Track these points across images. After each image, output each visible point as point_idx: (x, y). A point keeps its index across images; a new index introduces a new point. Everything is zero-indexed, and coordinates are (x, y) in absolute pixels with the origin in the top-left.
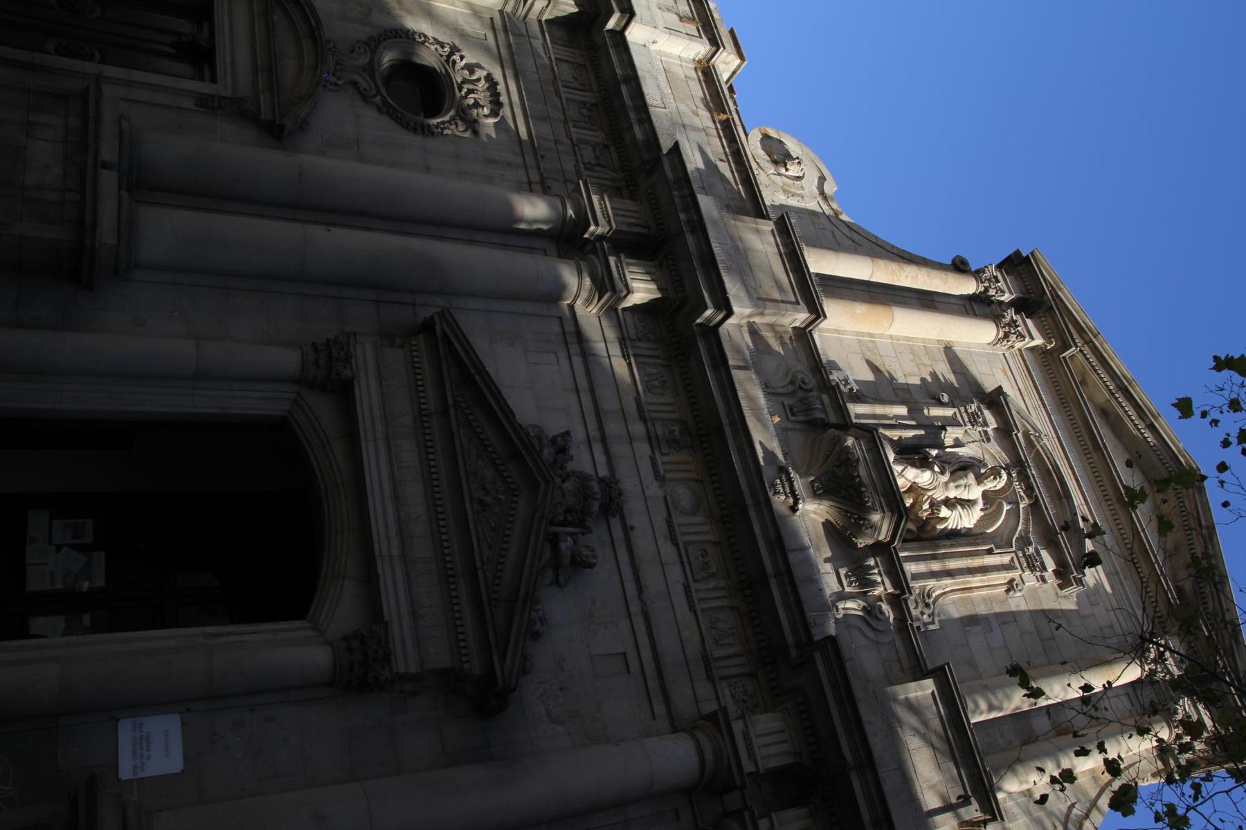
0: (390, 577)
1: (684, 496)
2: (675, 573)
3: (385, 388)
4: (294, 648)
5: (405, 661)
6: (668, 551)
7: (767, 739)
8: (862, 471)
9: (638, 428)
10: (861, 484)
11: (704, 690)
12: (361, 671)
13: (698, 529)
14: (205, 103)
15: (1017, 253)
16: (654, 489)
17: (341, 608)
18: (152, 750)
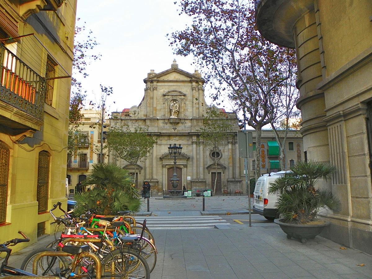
0: (180, 164)
1: (175, 138)
2: (181, 141)
3: (166, 162)
4: (184, 170)
5: (186, 163)
6: (179, 141)
7: (195, 139)
9: (168, 141)
11: (190, 141)
12: (186, 166)
13: (177, 138)
14: (140, 174)
15: (144, 80)
16: (174, 141)
17: (182, 166)
18: (189, 178)
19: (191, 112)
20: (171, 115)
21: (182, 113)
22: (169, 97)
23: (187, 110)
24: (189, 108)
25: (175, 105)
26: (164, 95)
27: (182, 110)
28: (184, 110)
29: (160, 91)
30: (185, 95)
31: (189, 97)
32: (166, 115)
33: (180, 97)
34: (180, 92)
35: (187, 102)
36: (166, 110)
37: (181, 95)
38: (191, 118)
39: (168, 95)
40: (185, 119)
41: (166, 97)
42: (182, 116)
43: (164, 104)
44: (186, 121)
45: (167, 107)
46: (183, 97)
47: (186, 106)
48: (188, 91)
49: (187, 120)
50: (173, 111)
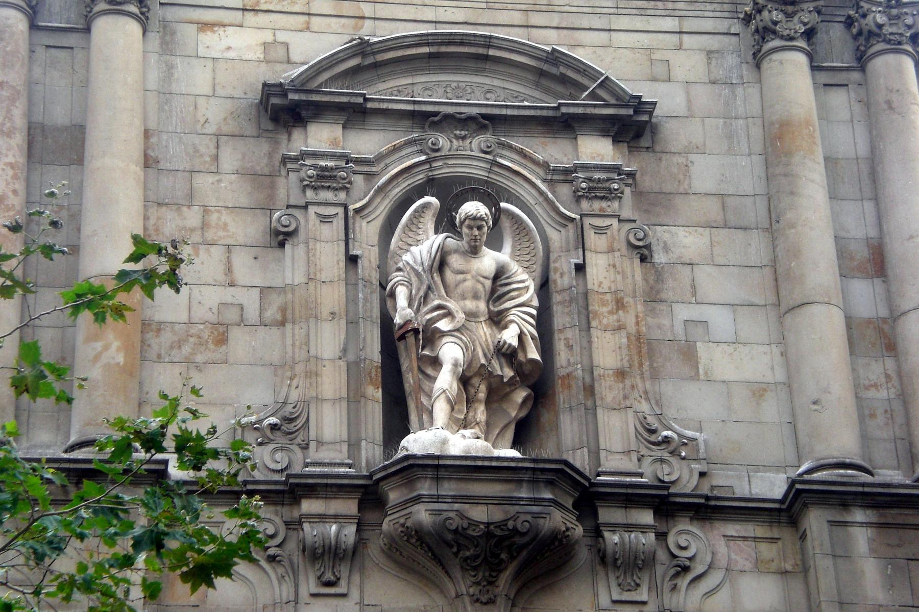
8: (479, 514)
10: (502, 524)
19: (759, 391)
20: (397, 422)
21: (608, 391)
22: (366, 142)
23: (689, 353)
24: (720, 320)
25: (488, 260)
26: (284, 109)
27: (608, 351)
28: (643, 348)
29: (214, 43)
30: (632, 125)
31: (706, 156)
32: (330, 423)
33: (554, 151)
34: (554, 70)
35: (681, 240)
36: (328, 340)
37: (565, 125)
38: (772, 486)
39: (356, 114)
40: (665, 504)
41: (321, 137)
42: (610, 445)
43: (281, 238)
44: (688, 537)
45: (332, 297)
46: (596, 150)
47: (653, 297)
48: (688, 64)
49: (708, 509)
50: (451, 352)
